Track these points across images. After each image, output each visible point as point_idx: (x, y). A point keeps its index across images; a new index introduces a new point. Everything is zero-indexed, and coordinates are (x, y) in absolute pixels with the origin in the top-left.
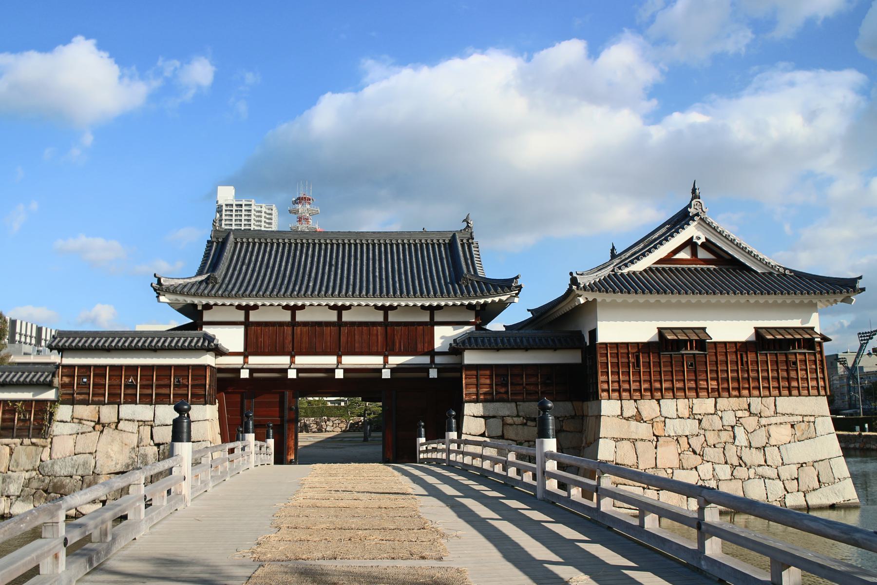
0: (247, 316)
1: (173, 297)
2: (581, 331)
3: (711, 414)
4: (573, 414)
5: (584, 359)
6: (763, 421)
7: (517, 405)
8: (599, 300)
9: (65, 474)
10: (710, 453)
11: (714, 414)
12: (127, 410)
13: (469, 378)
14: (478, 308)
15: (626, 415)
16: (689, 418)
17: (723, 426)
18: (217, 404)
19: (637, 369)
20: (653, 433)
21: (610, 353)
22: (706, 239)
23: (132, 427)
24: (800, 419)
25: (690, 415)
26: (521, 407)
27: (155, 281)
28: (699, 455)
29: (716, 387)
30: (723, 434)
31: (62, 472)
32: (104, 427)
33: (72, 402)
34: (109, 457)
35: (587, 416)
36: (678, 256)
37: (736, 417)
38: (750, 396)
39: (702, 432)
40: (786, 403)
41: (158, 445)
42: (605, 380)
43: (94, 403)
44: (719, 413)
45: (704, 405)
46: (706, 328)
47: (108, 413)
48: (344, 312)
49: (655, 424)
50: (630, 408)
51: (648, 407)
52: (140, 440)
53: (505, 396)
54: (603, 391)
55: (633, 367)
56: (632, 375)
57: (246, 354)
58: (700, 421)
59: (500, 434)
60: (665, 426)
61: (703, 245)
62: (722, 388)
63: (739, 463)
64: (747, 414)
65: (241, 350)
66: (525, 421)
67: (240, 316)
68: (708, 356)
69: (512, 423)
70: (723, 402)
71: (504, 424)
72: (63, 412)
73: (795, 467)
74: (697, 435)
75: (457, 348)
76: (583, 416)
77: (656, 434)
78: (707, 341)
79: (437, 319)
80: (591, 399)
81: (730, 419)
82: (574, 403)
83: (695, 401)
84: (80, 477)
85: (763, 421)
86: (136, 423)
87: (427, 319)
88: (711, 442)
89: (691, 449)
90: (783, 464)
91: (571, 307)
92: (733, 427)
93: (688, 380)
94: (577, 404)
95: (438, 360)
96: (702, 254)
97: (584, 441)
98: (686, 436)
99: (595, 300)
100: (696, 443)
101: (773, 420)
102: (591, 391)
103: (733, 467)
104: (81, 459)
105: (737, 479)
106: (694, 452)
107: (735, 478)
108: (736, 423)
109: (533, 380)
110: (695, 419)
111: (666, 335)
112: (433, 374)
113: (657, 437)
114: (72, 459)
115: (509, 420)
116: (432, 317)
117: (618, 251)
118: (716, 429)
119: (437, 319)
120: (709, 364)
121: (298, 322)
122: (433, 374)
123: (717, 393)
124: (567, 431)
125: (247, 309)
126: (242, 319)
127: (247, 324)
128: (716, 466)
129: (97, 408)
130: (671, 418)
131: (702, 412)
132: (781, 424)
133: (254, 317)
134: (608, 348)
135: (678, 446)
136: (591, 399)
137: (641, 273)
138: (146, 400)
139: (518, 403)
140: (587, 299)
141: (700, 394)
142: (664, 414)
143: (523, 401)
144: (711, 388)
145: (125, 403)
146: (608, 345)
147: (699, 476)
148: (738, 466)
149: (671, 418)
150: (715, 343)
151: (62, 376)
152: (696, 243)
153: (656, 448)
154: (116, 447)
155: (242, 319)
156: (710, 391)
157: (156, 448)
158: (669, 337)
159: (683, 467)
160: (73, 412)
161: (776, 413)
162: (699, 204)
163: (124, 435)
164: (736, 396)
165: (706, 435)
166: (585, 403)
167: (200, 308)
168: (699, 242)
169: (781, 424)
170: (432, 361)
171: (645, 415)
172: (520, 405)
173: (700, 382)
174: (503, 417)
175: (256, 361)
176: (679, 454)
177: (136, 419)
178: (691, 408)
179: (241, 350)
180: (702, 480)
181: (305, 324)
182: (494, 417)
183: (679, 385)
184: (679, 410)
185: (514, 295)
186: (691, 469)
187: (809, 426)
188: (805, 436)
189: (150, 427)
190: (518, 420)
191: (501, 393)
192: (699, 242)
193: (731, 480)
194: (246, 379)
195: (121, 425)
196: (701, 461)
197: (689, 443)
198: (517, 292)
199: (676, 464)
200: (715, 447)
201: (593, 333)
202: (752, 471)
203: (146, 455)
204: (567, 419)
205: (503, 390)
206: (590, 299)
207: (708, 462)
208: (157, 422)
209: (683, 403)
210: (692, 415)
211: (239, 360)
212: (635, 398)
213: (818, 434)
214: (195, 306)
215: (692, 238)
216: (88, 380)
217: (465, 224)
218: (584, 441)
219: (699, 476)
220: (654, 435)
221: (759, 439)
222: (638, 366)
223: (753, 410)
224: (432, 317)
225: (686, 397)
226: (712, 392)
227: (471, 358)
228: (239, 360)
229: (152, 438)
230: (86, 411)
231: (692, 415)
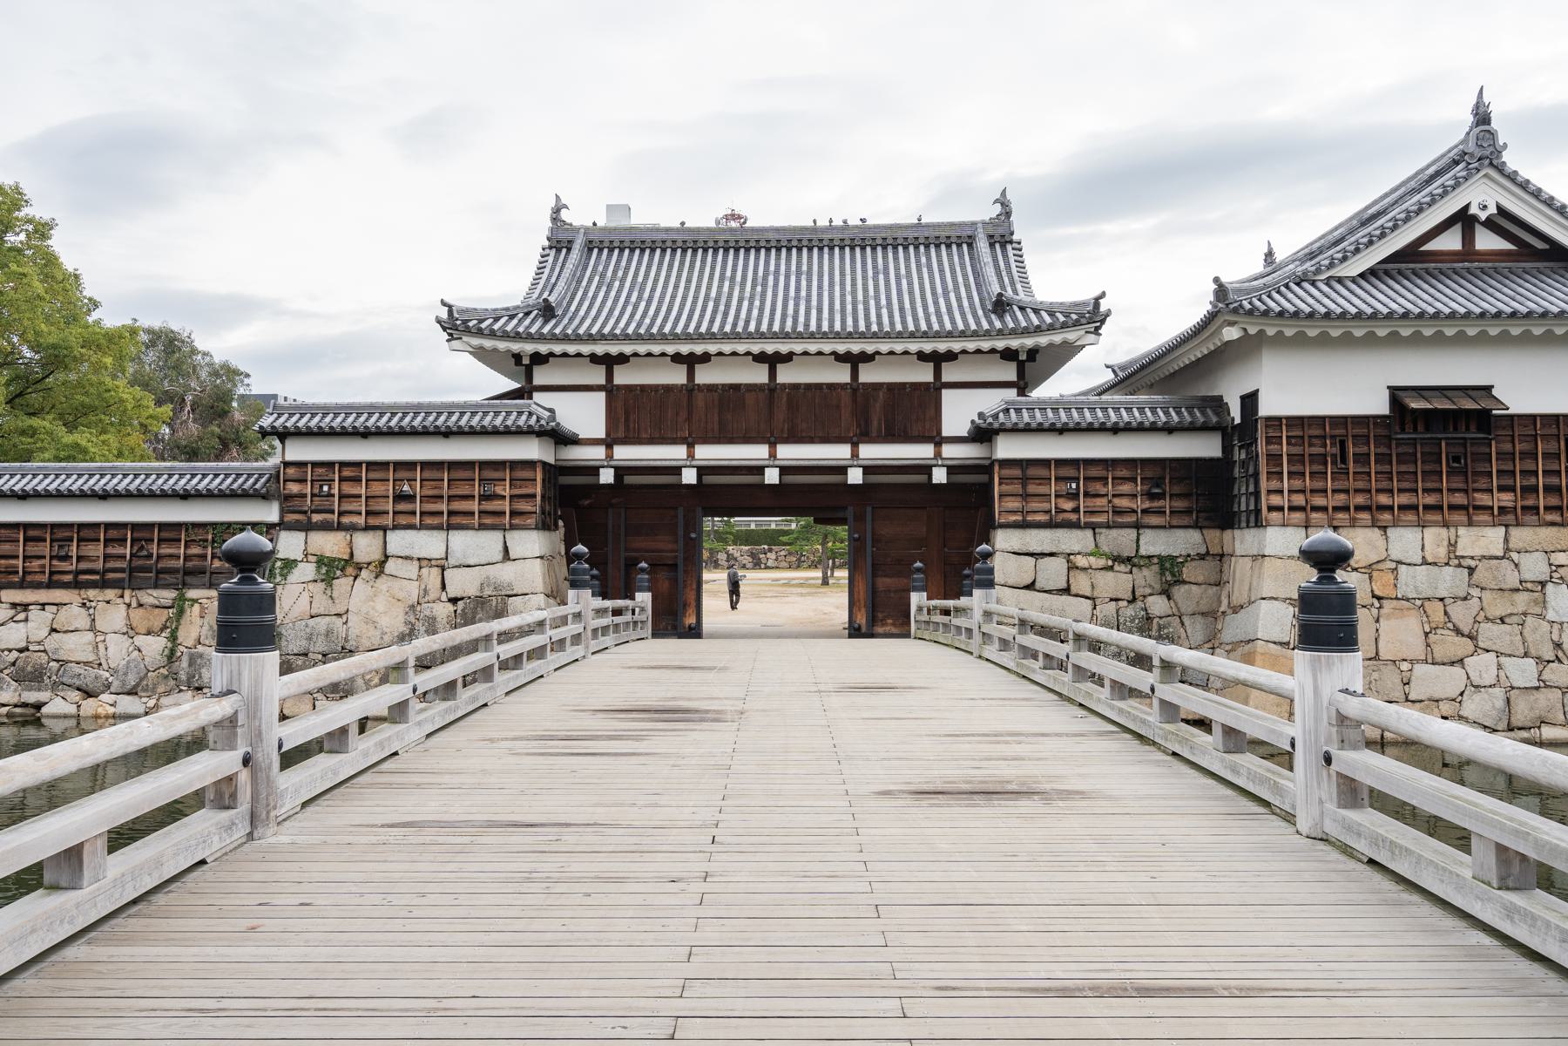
0: (610, 376)
1: (476, 341)
2: (1222, 396)
3: (1497, 558)
4: (1203, 550)
5: (1227, 448)
7: (1095, 534)
8: (1271, 332)
9: (296, 651)
10: (1488, 633)
11: (1503, 558)
12: (399, 541)
13: (1007, 484)
14: (1023, 357)
16: (1447, 564)
17: (1521, 582)
18: (562, 530)
19: (1341, 469)
20: (1372, 591)
21: (1287, 437)
22: (1499, 207)
23: (411, 569)
25: (1450, 558)
26: (1103, 537)
27: (444, 313)
28: (1470, 637)
29: (1510, 504)
30: (1522, 597)
31: (291, 647)
32: (361, 569)
33: (307, 527)
34: (370, 621)
35: (1232, 556)
37: (1550, 565)
39: (1475, 592)
41: (454, 601)
42: (1276, 490)
43: (340, 527)
45: (1483, 540)
46: (1493, 387)
47: (366, 546)
48: (780, 368)
49: (1375, 574)
52: (422, 592)
53: (1073, 517)
54: (1271, 509)
55: (1334, 463)
56: (1332, 479)
57: (609, 443)
58: (1471, 570)
59: (1063, 585)
60: (1396, 578)
61: (1490, 224)
62: (1523, 508)
63: (1557, 656)
65: (602, 435)
66: (1110, 563)
67: (597, 376)
68: (1493, 442)
69: (1087, 565)
70: (1520, 536)
71: (1072, 567)
74: (1465, 599)
75: (983, 434)
76: (1222, 555)
77: (1377, 592)
78: (1494, 412)
79: (946, 378)
80: (1244, 524)
81: (1535, 567)
82: (1205, 531)
83: (1462, 531)
84: (320, 657)
86: (416, 563)
89: (1450, 625)
91: (1208, 348)
92: (1543, 584)
93: (1449, 490)
94: (1212, 534)
95: (949, 451)
96: (1486, 241)
97: (1225, 602)
98: (1442, 600)
99: (1261, 332)
100: (1462, 615)
102: (1243, 507)
103: (1539, 659)
104: (322, 624)
105: (1551, 687)
106: (1458, 631)
107: (1547, 686)
108: (1551, 577)
109: (1126, 488)
110: (1460, 566)
111: (1407, 401)
112: (940, 476)
113: (1379, 598)
114: (307, 626)
115: (1081, 561)
116: (937, 373)
117: (1280, 256)
118: (1503, 586)
119: (946, 378)
120: (1497, 459)
121: (698, 385)
122: (940, 476)
123: (1505, 517)
124: (1190, 583)
125: (609, 362)
126: (602, 381)
127: (610, 389)
128: (1503, 659)
129: (348, 537)
130: (1409, 565)
131: (1478, 552)
133: (623, 377)
134: (1284, 427)
135: (1425, 619)
136: (1244, 524)
137: (1353, 280)
139: (1097, 530)
140: (1245, 330)
141: (1475, 518)
142: (1394, 557)
143: (1108, 527)
144: (1499, 508)
145: (395, 527)
146: (1284, 421)
147: (1468, 678)
148: (1553, 662)
149: (1409, 565)
150: (1512, 417)
151: (285, 481)
152: (1474, 218)
153: (1377, 621)
154: (380, 604)
155: (602, 381)
156: (1496, 512)
157: (451, 607)
158: (1414, 405)
159: (1433, 658)
160: (306, 543)
162: (1487, 135)
163: (396, 584)
164: (1553, 524)
165: (1483, 598)
166: (1228, 534)
167: (526, 361)
168: (1483, 216)
170: (938, 455)
172: (1100, 533)
173: (1475, 495)
174: (1069, 555)
175: (624, 453)
176: (1426, 634)
177: (416, 556)
178: (1452, 546)
179: (602, 435)
180: (1473, 686)
181: (711, 388)
182: (1052, 554)
183: (1430, 499)
184: (1426, 548)
185: (1093, 330)
186: (1452, 663)
189: (440, 570)
190: (1102, 562)
191: (1065, 511)
193: (1537, 688)
194: (610, 485)
195: (391, 566)
196: (1472, 648)
197: (1446, 613)
198: (1098, 324)
199: (1418, 650)
200: (1503, 622)
201: (1250, 401)
203: (434, 619)
204: (1192, 560)
205: (1069, 505)
206: (1252, 330)
207: (1488, 651)
208: (452, 561)
209: (1435, 539)
210: (1454, 557)
211: (598, 453)
212: (1336, 523)
214: (517, 358)
215: (1467, 207)
216: (330, 488)
217: (998, 208)
218: (1225, 602)
219: (1468, 678)
220: (1374, 596)
222: (1344, 460)
224: (937, 373)
225: (1446, 525)
226: (1499, 514)
227: (1007, 448)
228: (598, 453)
229: (444, 587)
230: (330, 544)
231: (1454, 557)
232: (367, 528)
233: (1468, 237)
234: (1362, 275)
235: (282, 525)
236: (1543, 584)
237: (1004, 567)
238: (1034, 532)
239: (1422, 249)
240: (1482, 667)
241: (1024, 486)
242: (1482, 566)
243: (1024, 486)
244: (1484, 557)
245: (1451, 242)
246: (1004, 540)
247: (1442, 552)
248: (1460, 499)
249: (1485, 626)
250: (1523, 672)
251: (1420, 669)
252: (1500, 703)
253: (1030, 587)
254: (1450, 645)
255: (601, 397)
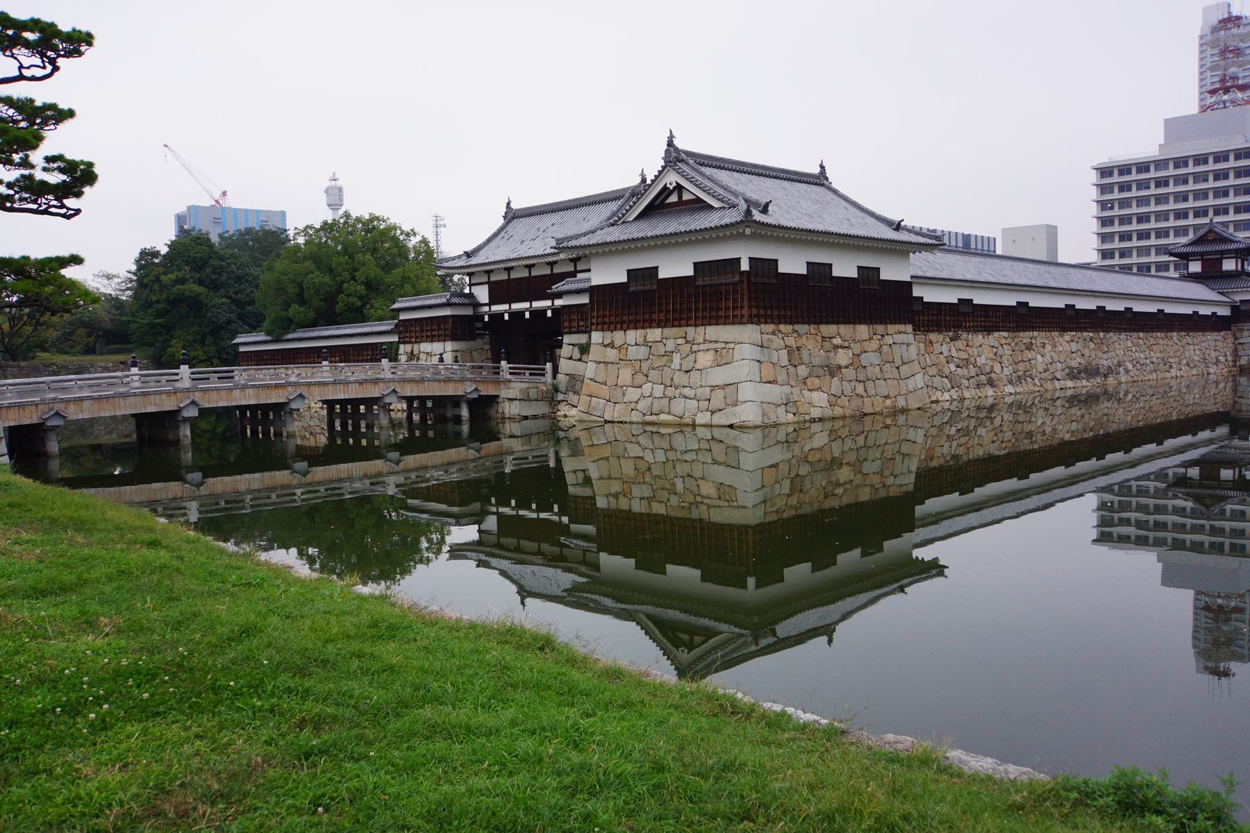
6: (695, 348)
15: (606, 343)
24: (723, 345)
30: (665, 358)
33: (404, 343)
36: (669, 201)
38: (687, 325)
40: (713, 331)
44: (664, 340)
46: (657, 268)
50: (608, 337)
51: (618, 337)
54: (592, 324)
57: (489, 304)
58: (650, 347)
64: (684, 341)
72: (402, 347)
73: (708, 389)
79: (578, 269)
81: (670, 345)
83: (648, 330)
85: (695, 348)
87: (573, 269)
88: (655, 365)
90: (701, 386)
92: (673, 352)
101: (702, 347)
103: (666, 386)
119: (578, 269)
123: (661, 324)
125: (488, 272)
126: (487, 280)
127: (489, 283)
132: (708, 350)
133: (494, 278)
138: (432, 339)
145: (421, 342)
155: (487, 280)
161: (705, 340)
169: (708, 350)
171: (618, 343)
175: (496, 308)
187: (727, 352)
188: (724, 362)
192: (671, 188)
199: (629, 382)
202: (678, 390)
205: (581, 324)
209: (640, 332)
210: (646, 343)
211: (486, 309)
213: (735, 359)
215: (666, 185)
221: (688, 364)
223: (688, 338)
228: (486, 309)
230: (408, 347)
231: (646, 343)
232: (416, 342)
233: (680, 196)
234: (636, 219)
235: (399, 343)
236: (673, 352)
237: (565, 351)
238: (573, 335)
239: (667, 202)
240: (647, 388)
241: (570, 316)
242: (654, 345)
243: (570, 316)
244: (654, 342)
245: (673, 198)
246: (567, 339)
247: (642, 339)
248: (647, 317)
249: (651, 371)
250: (659, 390)
251: (630, 389)
252: (649, 404)
253: (571, 358)
254: (640, 378)
255: (486, 286)
